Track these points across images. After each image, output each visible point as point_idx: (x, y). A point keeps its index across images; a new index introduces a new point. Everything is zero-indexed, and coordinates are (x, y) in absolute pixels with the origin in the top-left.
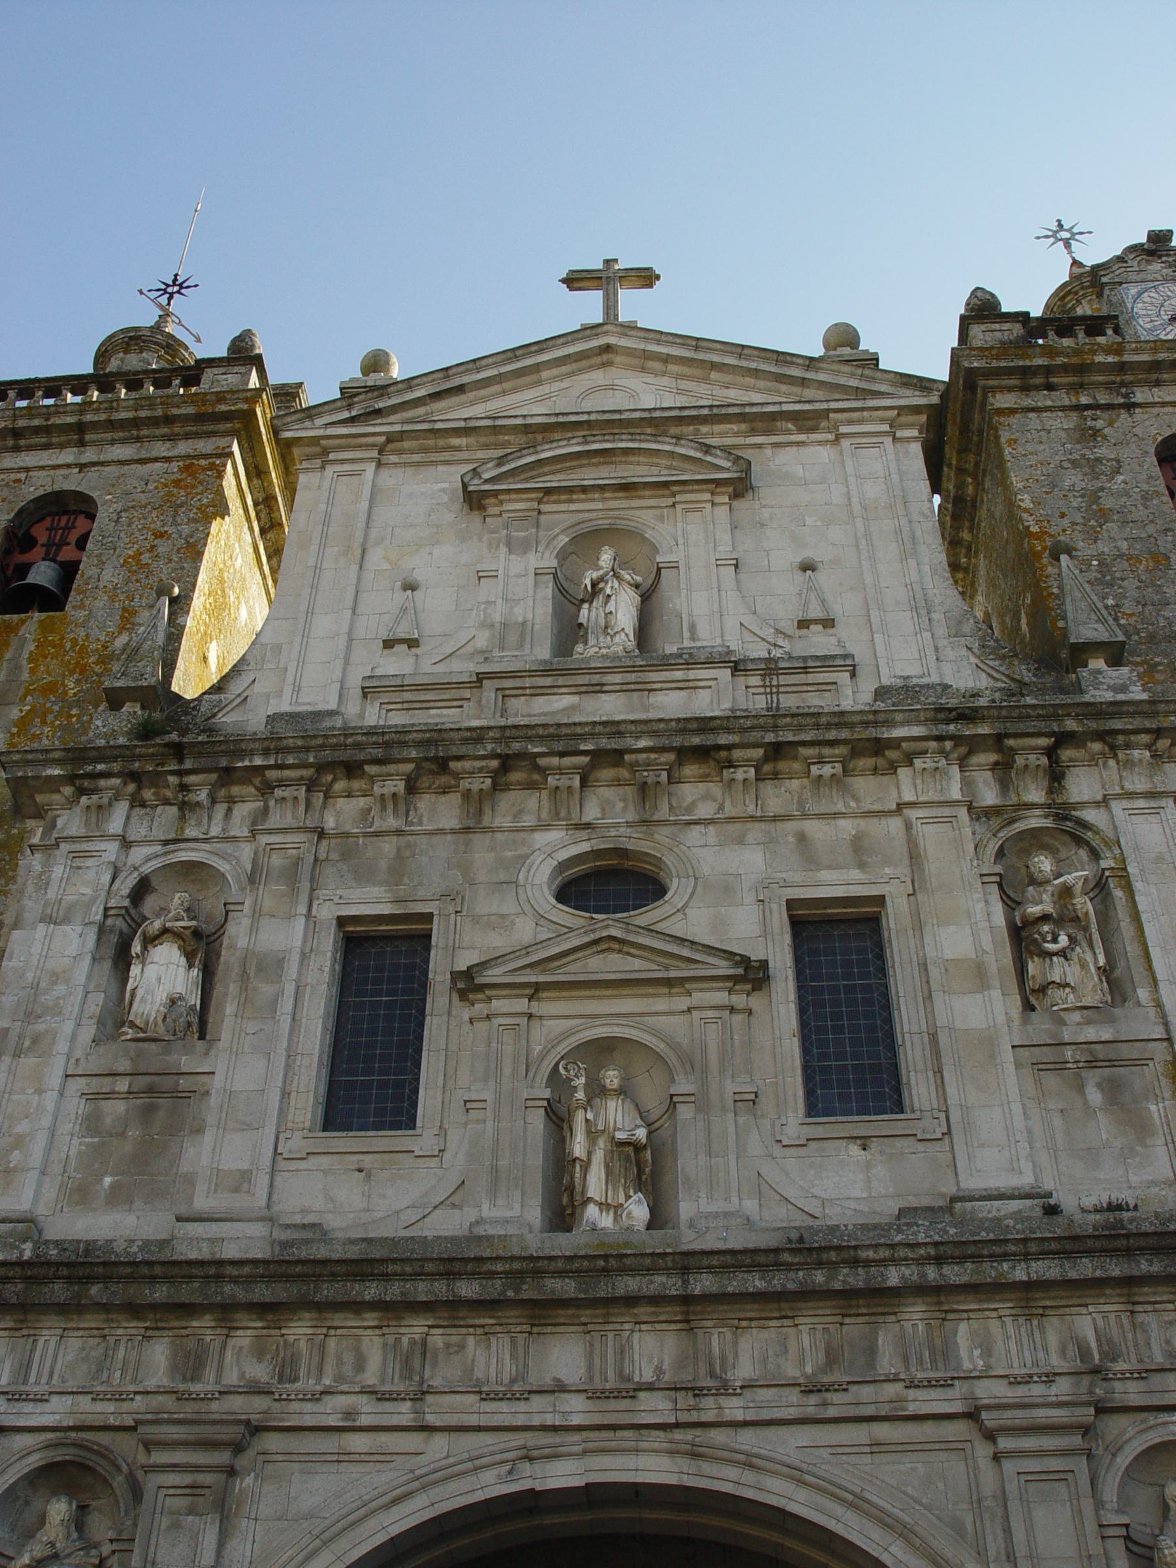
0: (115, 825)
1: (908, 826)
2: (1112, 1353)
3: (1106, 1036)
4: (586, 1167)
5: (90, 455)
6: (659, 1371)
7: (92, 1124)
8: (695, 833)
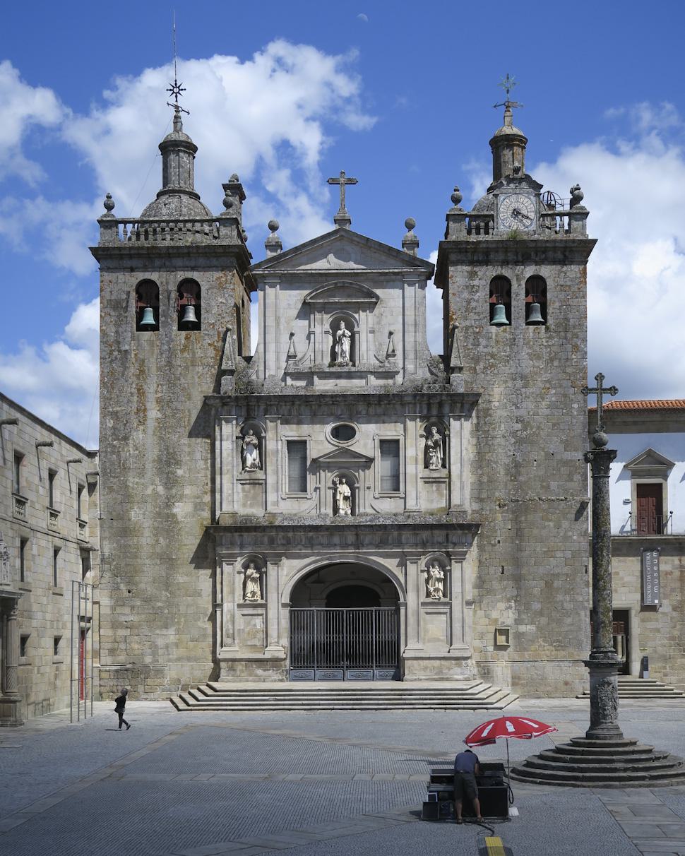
2: (427, 542)
3: (439, 476)
7: (243, 490)
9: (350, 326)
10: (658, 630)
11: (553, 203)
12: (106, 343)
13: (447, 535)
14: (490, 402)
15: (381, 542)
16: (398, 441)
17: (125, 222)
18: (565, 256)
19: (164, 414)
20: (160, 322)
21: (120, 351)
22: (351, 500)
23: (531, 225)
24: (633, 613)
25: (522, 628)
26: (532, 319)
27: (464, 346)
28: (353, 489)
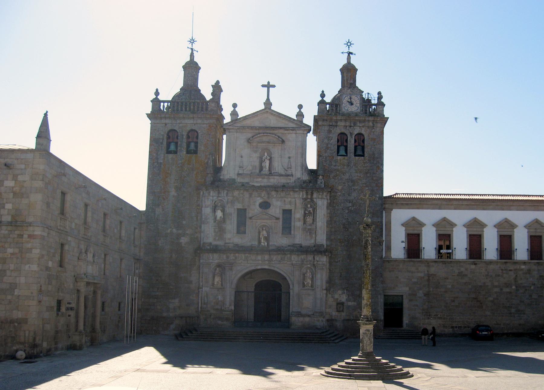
0: (211, 195)
1: (295, 200)
4: (262, 238)
5: (195, 122)
6: (267, 259)
7: (215, 232)
8: (274, 199)
9: (270, 154)
10: (417, 306)
11: (370, 98)
12: (151, 159)
13: (314, 257)
14: (337, 193)
15: (281, 259)
16: (291, 210)
17: (164, 102)
18: (373, 124)
19: (178, 193)
20: (178, 149)
21: (158, 163)
22: (267, 239)
23: (358, 109)
24: (404, 297)
25: (350, 304)
26: (357, 154)
27: (324, 165)
28: (268, 233)
